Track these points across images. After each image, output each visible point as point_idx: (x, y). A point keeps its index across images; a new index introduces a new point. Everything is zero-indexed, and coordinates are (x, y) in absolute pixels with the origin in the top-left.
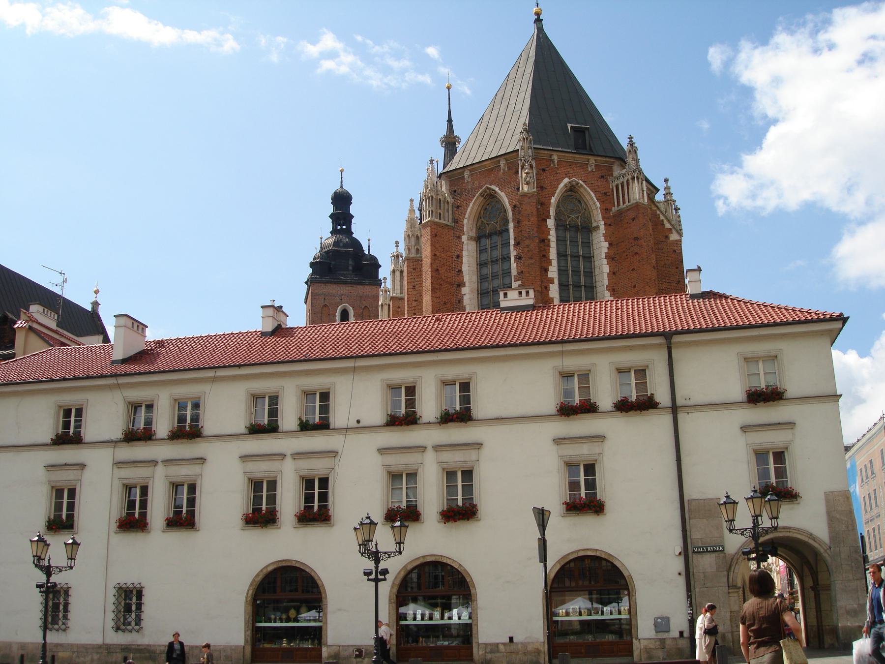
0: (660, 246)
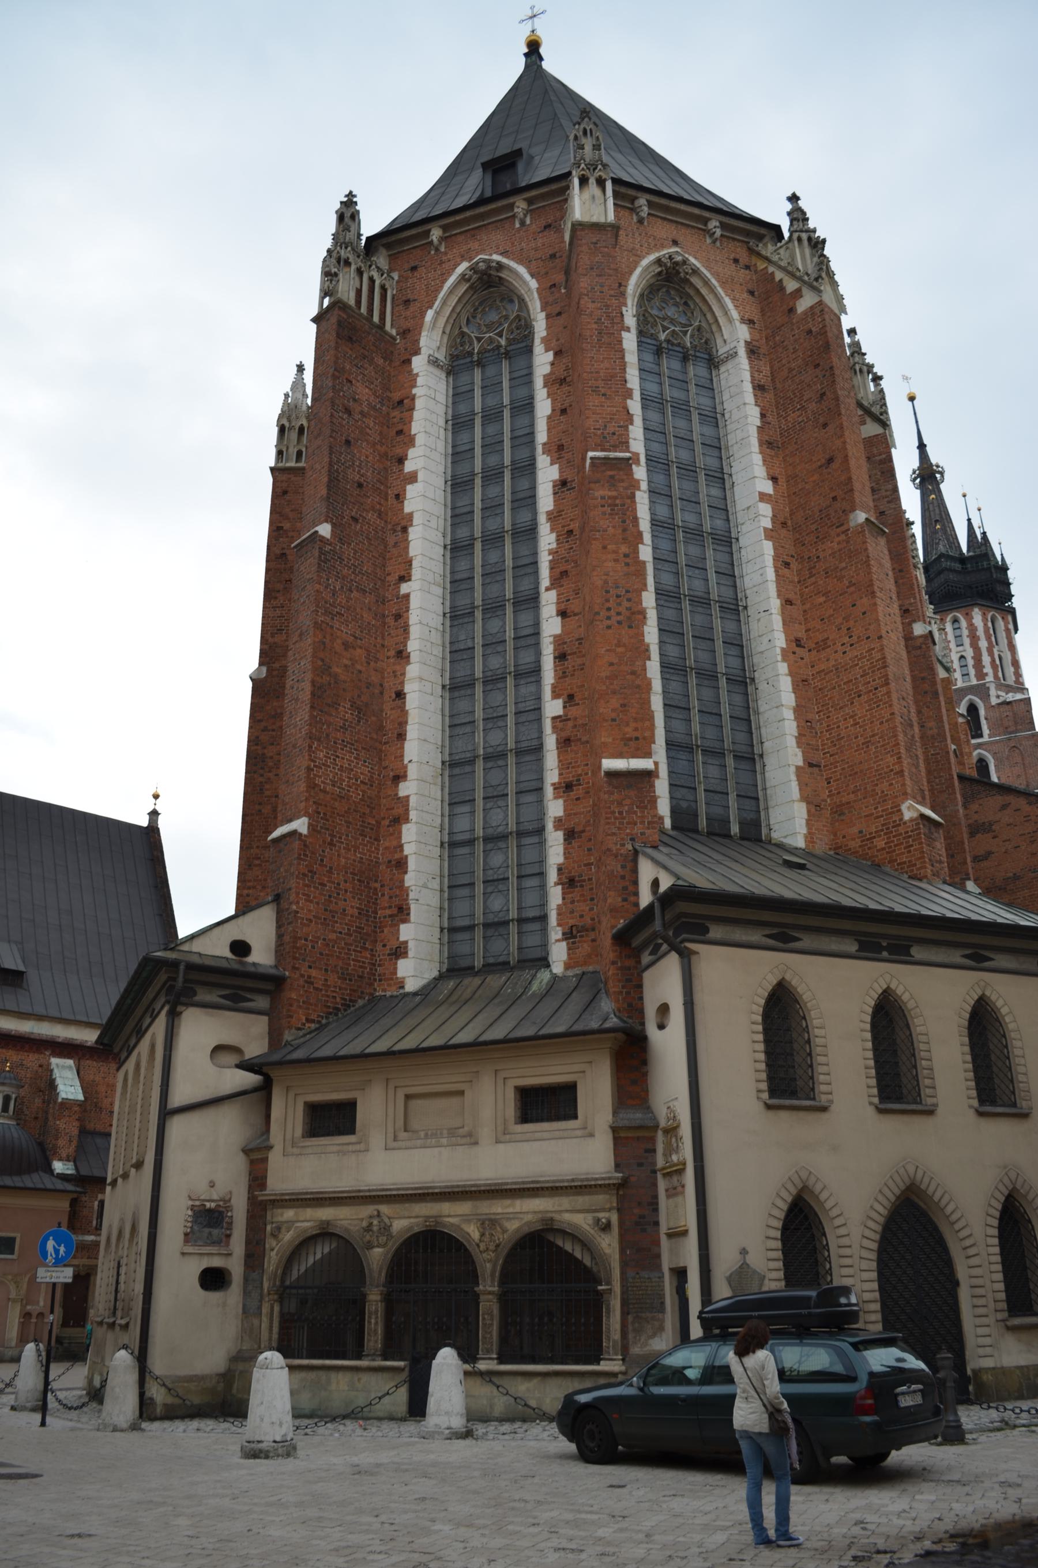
0: (777, 338)
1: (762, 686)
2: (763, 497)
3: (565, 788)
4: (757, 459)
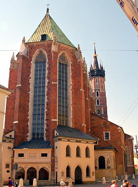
1: (69, 108)
2: (71, 85)
3: (47, 120)
4: (71, 80)
